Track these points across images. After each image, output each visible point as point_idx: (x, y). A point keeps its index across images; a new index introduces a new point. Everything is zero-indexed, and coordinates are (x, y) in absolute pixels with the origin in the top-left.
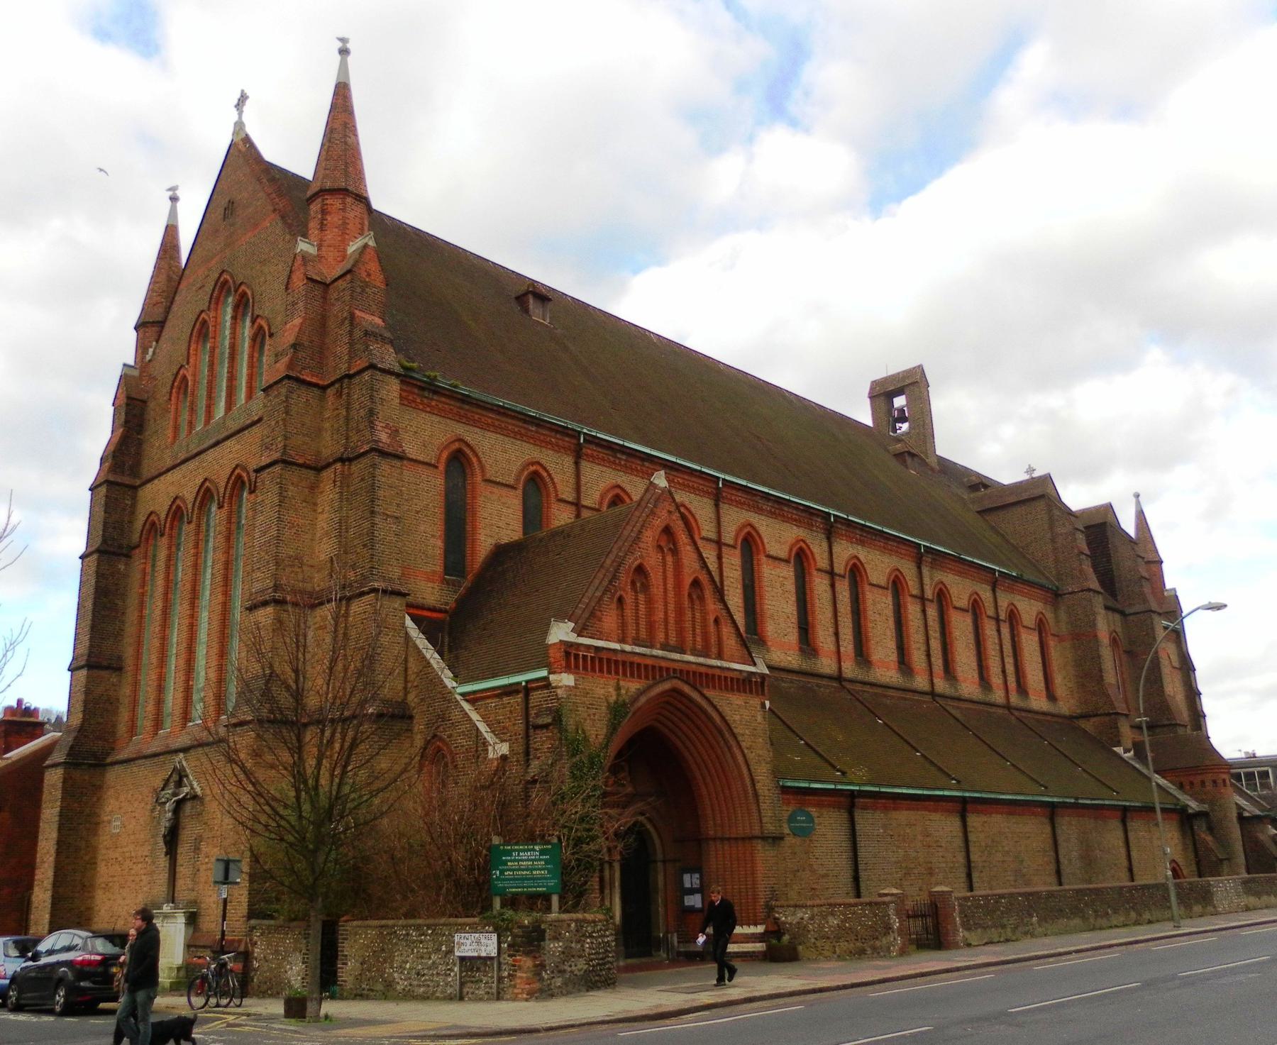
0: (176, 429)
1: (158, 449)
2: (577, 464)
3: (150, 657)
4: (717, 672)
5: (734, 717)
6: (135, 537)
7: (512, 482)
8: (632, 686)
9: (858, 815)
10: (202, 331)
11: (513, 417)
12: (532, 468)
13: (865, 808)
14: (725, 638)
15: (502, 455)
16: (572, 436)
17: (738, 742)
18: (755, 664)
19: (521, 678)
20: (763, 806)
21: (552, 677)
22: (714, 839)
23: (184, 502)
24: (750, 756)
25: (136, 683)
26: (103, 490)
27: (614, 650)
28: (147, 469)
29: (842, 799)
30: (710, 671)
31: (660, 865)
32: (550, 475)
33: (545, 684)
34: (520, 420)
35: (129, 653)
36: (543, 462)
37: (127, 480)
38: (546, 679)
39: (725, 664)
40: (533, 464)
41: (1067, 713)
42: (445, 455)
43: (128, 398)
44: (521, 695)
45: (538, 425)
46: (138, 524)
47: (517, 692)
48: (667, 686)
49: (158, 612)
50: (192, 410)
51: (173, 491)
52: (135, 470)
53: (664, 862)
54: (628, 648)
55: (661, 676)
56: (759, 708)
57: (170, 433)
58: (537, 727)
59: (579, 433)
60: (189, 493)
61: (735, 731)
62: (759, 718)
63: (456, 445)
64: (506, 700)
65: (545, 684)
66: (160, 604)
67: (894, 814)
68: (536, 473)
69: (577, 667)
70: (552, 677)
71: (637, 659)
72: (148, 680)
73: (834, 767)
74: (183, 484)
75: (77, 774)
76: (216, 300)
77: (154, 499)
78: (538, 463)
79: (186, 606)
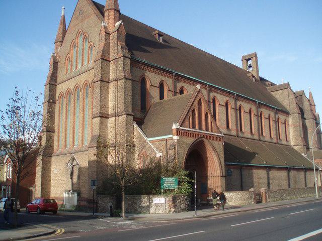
0: (67, 70)
1: (61, 75)
3: (62, 129)
6: (57, 98)
10: (74, 45)
23: (70, 89)
25: (59, 136)
26: (48, 86)
28: (59, 80)
35: (56, 128)
37: (54, 83)
43: (54, 62)
46: (57, 95)
49: (64, 118)
50: (72, 65)
51: (67, 87)
52: (56, 81)
57: (65, 71)
60: (72, 87)
66: (65, 116)
72: (62, 135)
74: (71, 85)
75: (45, 158)
76: (77, 37)
77: (61, 88)
79: (72, 116)
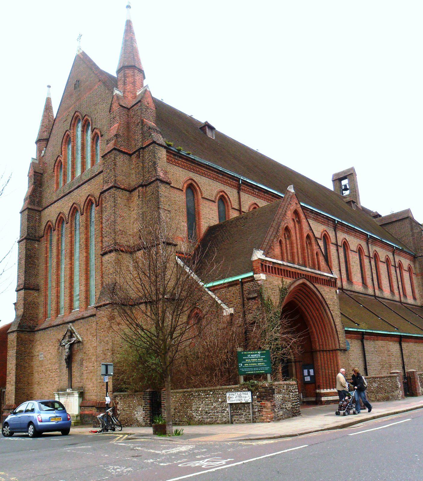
2: (239, 193)
4: (319, 276)
5: (326, 297)
7: (213, 199)
8: (288, 281)
9: (365, 342)
11: (212, 171)
12: (221, 194)
13: (367, 339)
14: (320, 261)
15: (209, 187)
16: (236, 180)
17: (329, 308)
18: (332, 274)
19: (239, 278)
20: (340, 336)
21: (255, 276)
22: (319, 351)
24: (333, 314)
27: (280, 264)
29: (359, 336)
30: (317, 276)
31: (293, 364)
32: (228, 197)
33: (252, 279)
34: (215, 172)
36: (225, 191)
38: (252, 277)
39: (322, 273)
40: (221, 192)
41: (420, 305)
42: (185, 186)
44: (240, 285)
45: (222, 175)
47: (236, 284)
48: (301, 281)
53: (295, 362)
54: (285, 263)
55: (298, 277)
56: (335, 292)
58: (249, 299)
59: (239, 179)
61: (327, 303)
62: (335, 297)
63: (190, 182)
64: (230, 288)
65: (252, 279)
67: (377, 342)
68: (222, 196)
69: (266, 271)
70: (255, 276)
71: (289, 269)
73: (354, 322)
78: (223, 191)
